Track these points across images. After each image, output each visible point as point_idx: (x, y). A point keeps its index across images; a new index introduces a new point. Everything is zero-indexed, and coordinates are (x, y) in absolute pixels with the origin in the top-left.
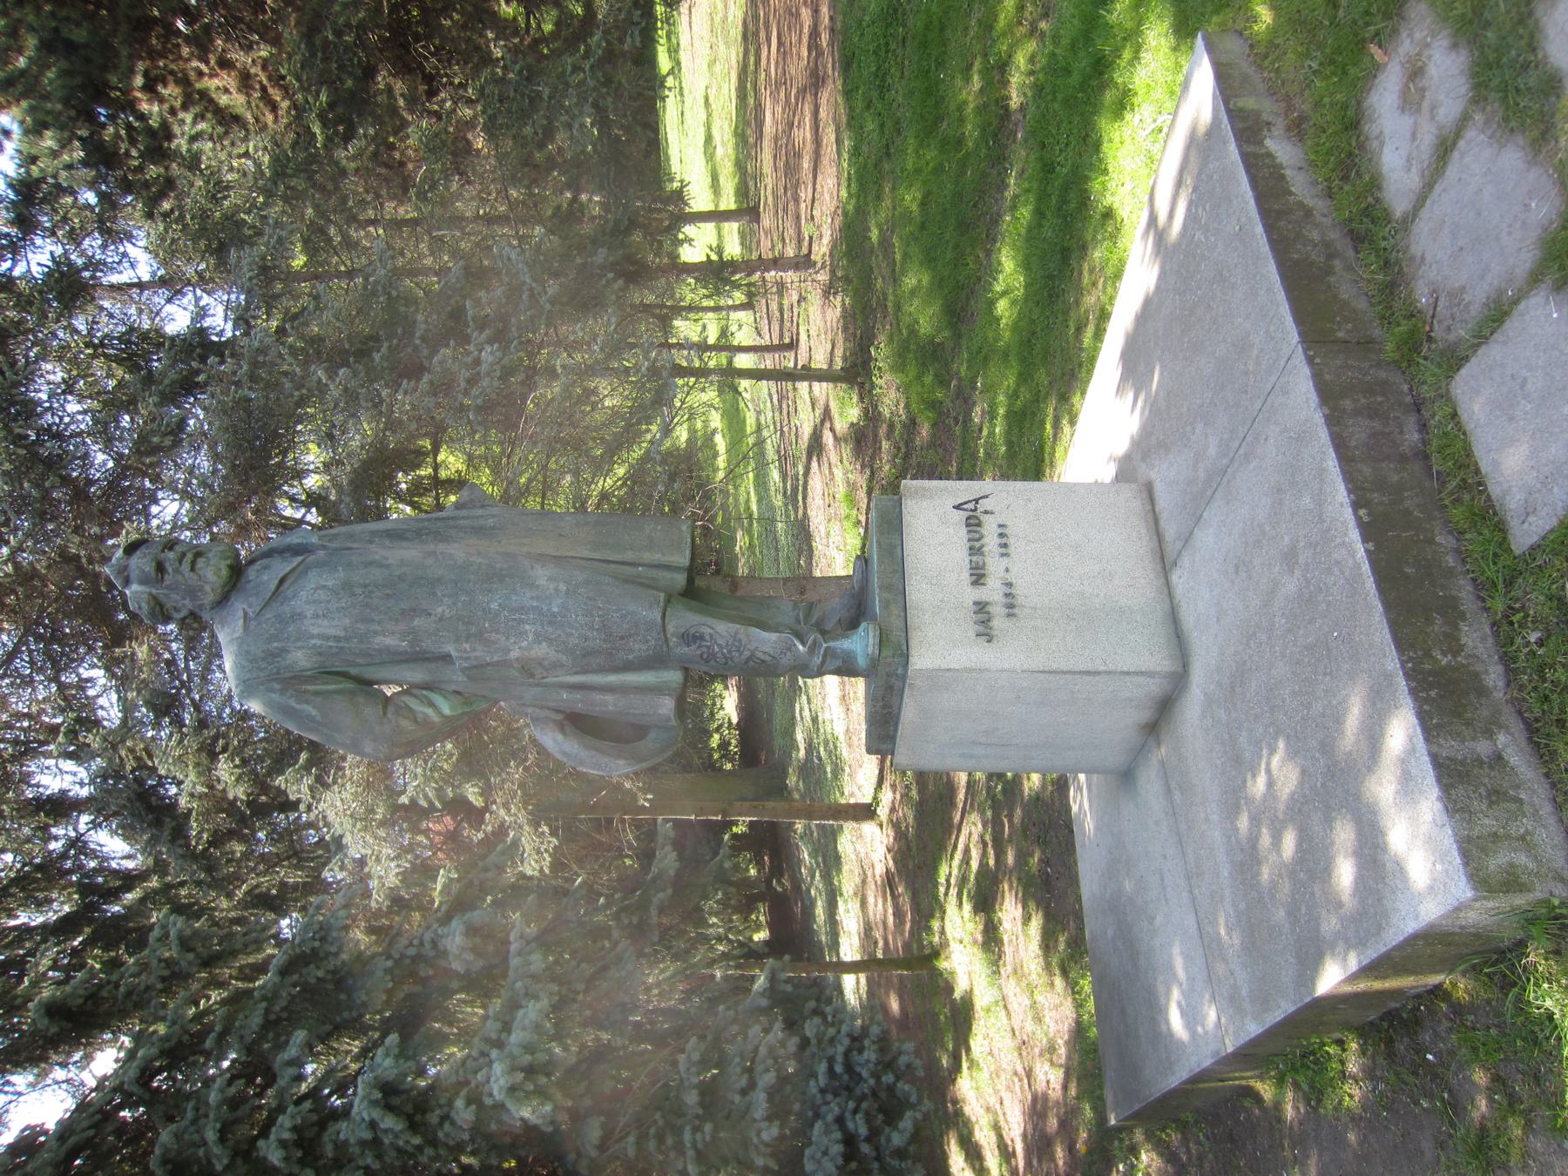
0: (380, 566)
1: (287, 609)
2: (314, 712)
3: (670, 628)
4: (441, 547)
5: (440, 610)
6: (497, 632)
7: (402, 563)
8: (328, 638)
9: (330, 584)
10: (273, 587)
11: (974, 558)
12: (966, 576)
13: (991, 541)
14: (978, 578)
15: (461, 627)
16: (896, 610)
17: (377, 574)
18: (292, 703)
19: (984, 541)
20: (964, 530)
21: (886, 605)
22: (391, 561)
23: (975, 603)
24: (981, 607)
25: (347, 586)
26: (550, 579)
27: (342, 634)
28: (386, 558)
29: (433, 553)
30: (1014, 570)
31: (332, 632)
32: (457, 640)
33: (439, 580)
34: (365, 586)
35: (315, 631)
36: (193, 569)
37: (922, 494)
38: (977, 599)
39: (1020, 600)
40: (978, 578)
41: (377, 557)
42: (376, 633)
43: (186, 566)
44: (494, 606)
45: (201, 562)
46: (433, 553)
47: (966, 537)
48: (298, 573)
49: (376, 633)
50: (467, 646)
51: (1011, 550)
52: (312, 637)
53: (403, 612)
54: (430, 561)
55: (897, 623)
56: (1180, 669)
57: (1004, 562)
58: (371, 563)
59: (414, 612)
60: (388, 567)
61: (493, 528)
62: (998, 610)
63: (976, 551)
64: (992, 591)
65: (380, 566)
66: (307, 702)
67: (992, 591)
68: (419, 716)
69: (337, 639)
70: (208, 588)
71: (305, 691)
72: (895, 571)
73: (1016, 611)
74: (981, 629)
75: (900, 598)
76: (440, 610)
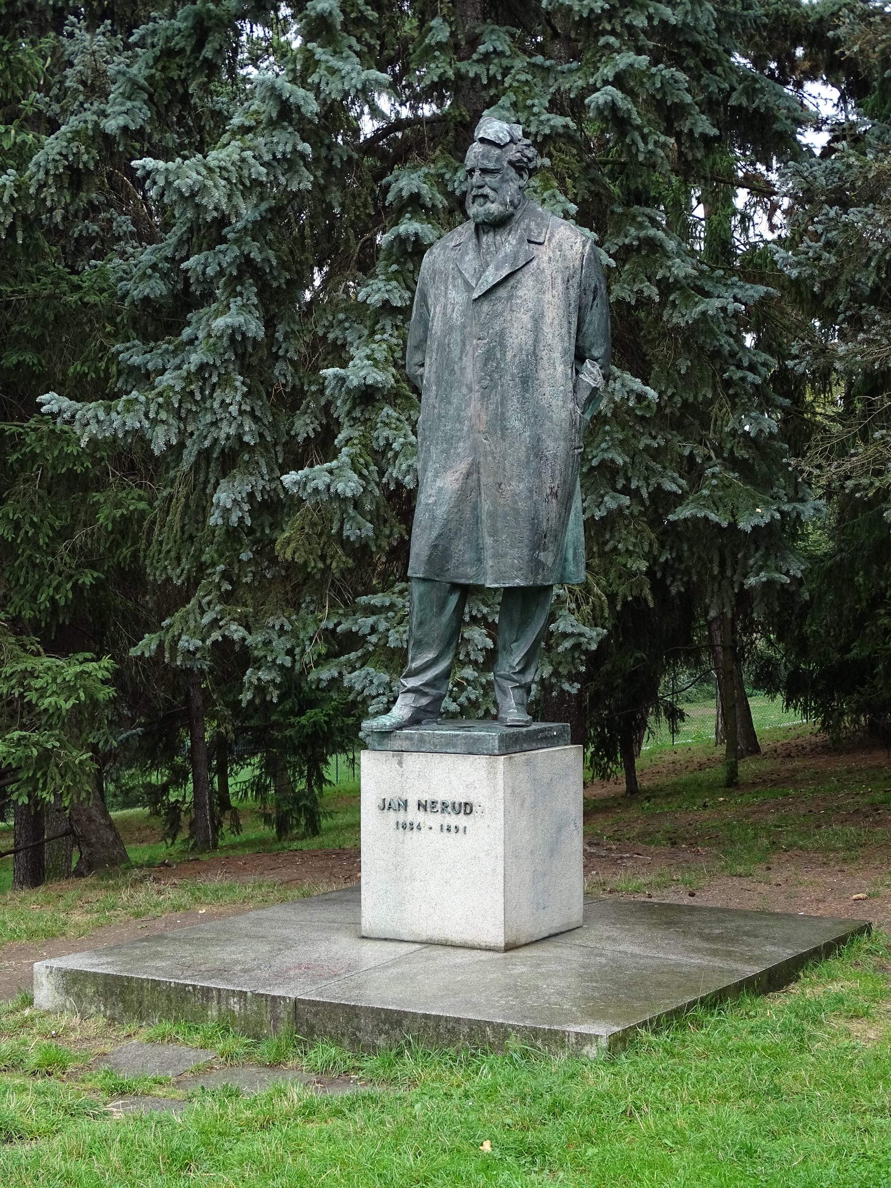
0: (462, 352)
7: (463, 369)
12: (426, 797)
13: (452, 820)
14: (422, 806)
16: (406, 744)
17: (456, 352)
19: (453, 816)
20: (463, 801)
21: (409, 738)
26: (440, 489)
29: (470, 390)
30: (431, 833)
33: (449, 403)
37: (492, 771)
38: (409, 803)
39: (408, 833)
40: (422, 806)
45: (482, 200)
46: (470, 390)
54: (464, 390)
56: (364, 934)
58: (464, 344)
60: (461, 359)
61: (504, 428)
62: (401, 817)
64: (413, 815)
67: (413, 815)
72: (435, 746)
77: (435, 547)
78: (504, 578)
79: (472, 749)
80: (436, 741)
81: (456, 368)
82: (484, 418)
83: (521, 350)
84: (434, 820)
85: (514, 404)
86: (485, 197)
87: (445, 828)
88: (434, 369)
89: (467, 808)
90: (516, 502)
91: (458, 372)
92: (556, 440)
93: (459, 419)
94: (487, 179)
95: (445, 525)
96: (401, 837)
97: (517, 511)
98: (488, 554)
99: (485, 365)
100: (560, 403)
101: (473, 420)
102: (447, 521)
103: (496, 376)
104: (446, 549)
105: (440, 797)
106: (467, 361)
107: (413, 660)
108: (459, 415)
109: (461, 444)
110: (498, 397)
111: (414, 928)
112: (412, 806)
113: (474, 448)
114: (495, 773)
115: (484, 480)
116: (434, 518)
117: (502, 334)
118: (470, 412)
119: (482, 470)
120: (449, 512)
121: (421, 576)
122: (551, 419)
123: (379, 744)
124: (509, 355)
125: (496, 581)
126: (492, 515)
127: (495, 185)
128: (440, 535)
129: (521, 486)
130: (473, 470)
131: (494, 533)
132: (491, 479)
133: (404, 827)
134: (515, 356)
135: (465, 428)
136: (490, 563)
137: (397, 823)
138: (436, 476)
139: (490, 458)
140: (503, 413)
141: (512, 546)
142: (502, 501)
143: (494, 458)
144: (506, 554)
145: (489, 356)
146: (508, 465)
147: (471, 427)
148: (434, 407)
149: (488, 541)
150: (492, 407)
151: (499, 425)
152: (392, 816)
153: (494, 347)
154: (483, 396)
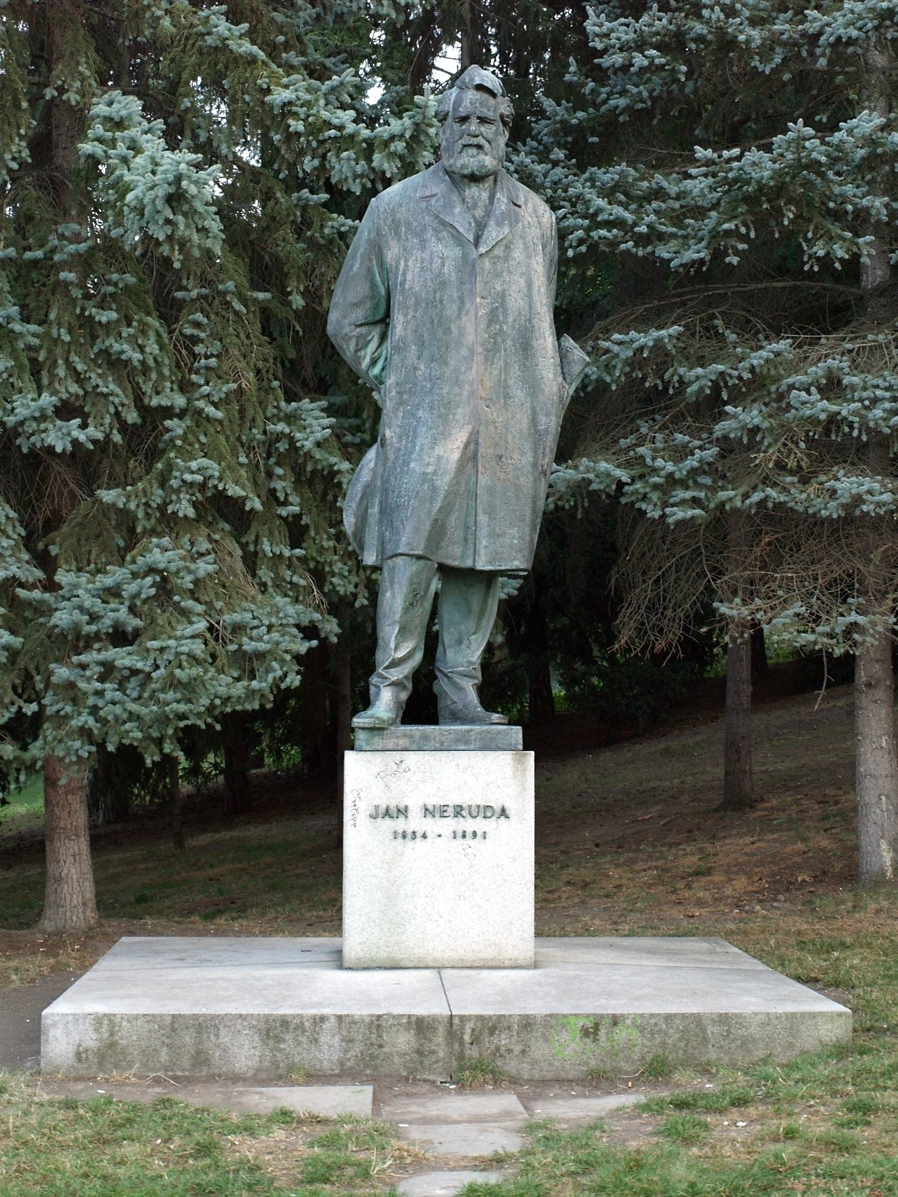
0: (460, 310)
1: (429, 234)
2: (355, 269)
3: (399, 561)
4: (478, 359)
5: (422, 367)
6: (403, 417)
7: (462, 330)
8: (404, 275)
9: (446, 269)
10: (448, 219)
12: (431, 802)
13: (470, 825)
14: (428, 811)
15: (408, 386)
16: (403, 742)
17: (451, 310)
18: (362, 250)
20: (482, 803)
22: (464, 318)
23: (406, 807)
24: (403, 812)
25: (443, 285)
27: (407, 287)
28: (467, 314)
29: (472, 352)
31: (409, 277)
32: (398, 384)
33: (446, 363)
34: (441, 302)
35: (410, 263)
36: (465, 146)
38: (410, 808)
39: (409, 844)
40: (428, 811)
41: (468, 305)
42: (406, 315)
43: (466, 140)
44: (420, 413)
45: (474, 151)
47: (473, 803)
48: (458, 238)
49: (406, 315)
50: (393, 393)
51: (460, 841)
52: (406, 261)
53: (421, 336)
56: (346, 964)
57: (447, 833)
59: (421, 344)
60: (459, 317)
61: (507, 396)
62: (400, 824)
63: (459, 811)
65: (460, 310)
66: (362, 263)
67: (416, 822)
68: (362, 353)
70: (452, 161)
71: (371, 260)
72: (442, 743)
73: (400, 840)
74: (382, 810)
75: (415, 747)
76: (422, 367)
77: (436, 520)
79: (488, 745)
80: (443, 739)
81: (453, 326)
82: (488, 384)
83: (520, 314)
84: (448, 825)
85: (515, 370)
86: (479, 147)
87: (460, 834)
88: (411, 326)
90: (518, 478)
91: (455, 331)
92: (547, 415)
93: (457, 382)
94: (482, 129)
95: (445, 497)
96: (400, 849)
97: (518, 487)
98: (483, 532)
99: (489, 326)
100: (551, 376)
101: (475, 386)
102: (448, 493)
103: (499, 339)
104: (444, 525)
105: (453, 799)
106: (468, 322)
107: (396, 648)
108: (457, 378)
109: (460, 410)
110: (502, 362)
111: (416, 951)
112: (415, 812)
113: (476, 416)
114: (524, 770)
115: (482, 450)
116: (434, 489)
117: (503, 295)
118: (472, 375)
119: (481, 440)
120: (450, 485)
121: (420, 552)
122: (543, 391)
123: (368, 744)
124: (510, 319)
126: (491, 491)
127: (490, 136)
128: (441, 508)
129: (524, 460)
130: (473, 441)
131: (491, 512)
132: (491, 451)
133: (404, 837)
134: (515, 320)
135: (465, 394)
136: (484, 543)
137: (395, 832)
138: (434, 443)
139: (491, 428)
140: (505, 380)
141: (512, 526)
142: (502, 476)
143: (496, 428)
144: (504, 534)
145: (493, 318)
146: (510, 437)
147: (472, 393)
148: (415, 369)
149: (483, 518)
150: (496, 372)
151: (503, 392)
152: (388, 825)
153: (497, 308)
154: (486, 359)
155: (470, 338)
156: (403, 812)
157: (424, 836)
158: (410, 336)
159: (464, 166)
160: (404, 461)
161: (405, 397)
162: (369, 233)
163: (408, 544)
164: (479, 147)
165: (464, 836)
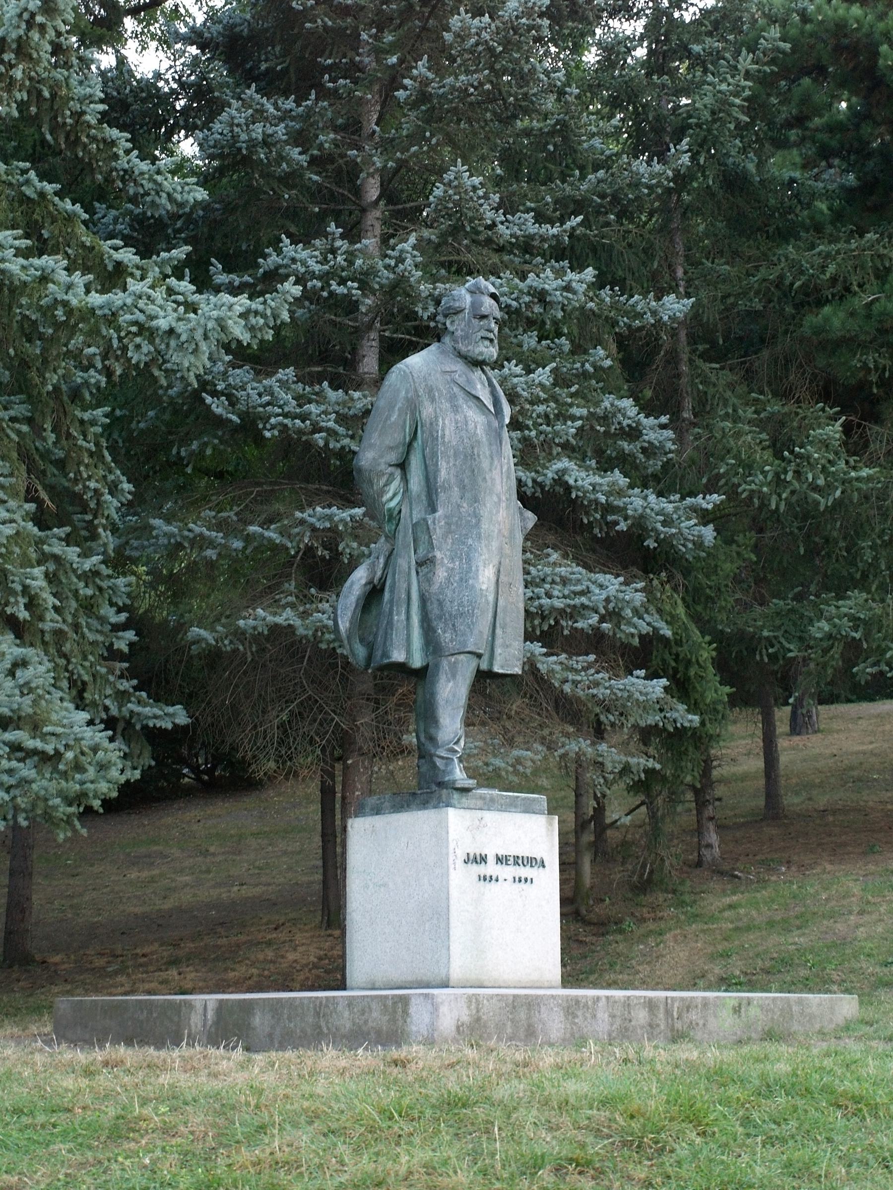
2: (393, 419)
5: (465, 505)
6: (453, 543)
7: (493, 480)
8: (443, 430)
11: (512, 859)
12: (502, 852)
14: (499, 860)
15: (455, 519)
16: (480, 803)
17: (485, 464)
18: (399, 405)
21: (482, 798)
24: (483, 859)
29: (500, 500)
31: (447, 432)
32: (446, 517)
34: (479, 456)
40: (499, 860)
41: (496, 462)
42: (448, 463)
45: (487, 343)
46: (500, 500)
47: (525, 855)
52: (443, 420)
53: (462, 481)
54: (495, 499)
55: (471, 802)
59: (463, 488)
60: (490, 470)
62: (482, 869)
64: (492, 868)
65: (491, 464)
66: (399, 415)
67: (492, 868)
69: (443, 436)
74: (471, 857)
76: (465, 505)
78: (508, 666)
79: (528, 809)
89: (532, 862)
106: (496, 474)
112: (491, 859)
125: (502, 667)
133: (485, 879)
155: (498, 487)
156: (483, 859)
157: (497, 880)
158: (453, 480)
159: (481, 353)
160: (461, 579)
161: (453, 527)
162: (407, 392)
163: (476, 644)
164: (491, 341)
165: (520, 881)
